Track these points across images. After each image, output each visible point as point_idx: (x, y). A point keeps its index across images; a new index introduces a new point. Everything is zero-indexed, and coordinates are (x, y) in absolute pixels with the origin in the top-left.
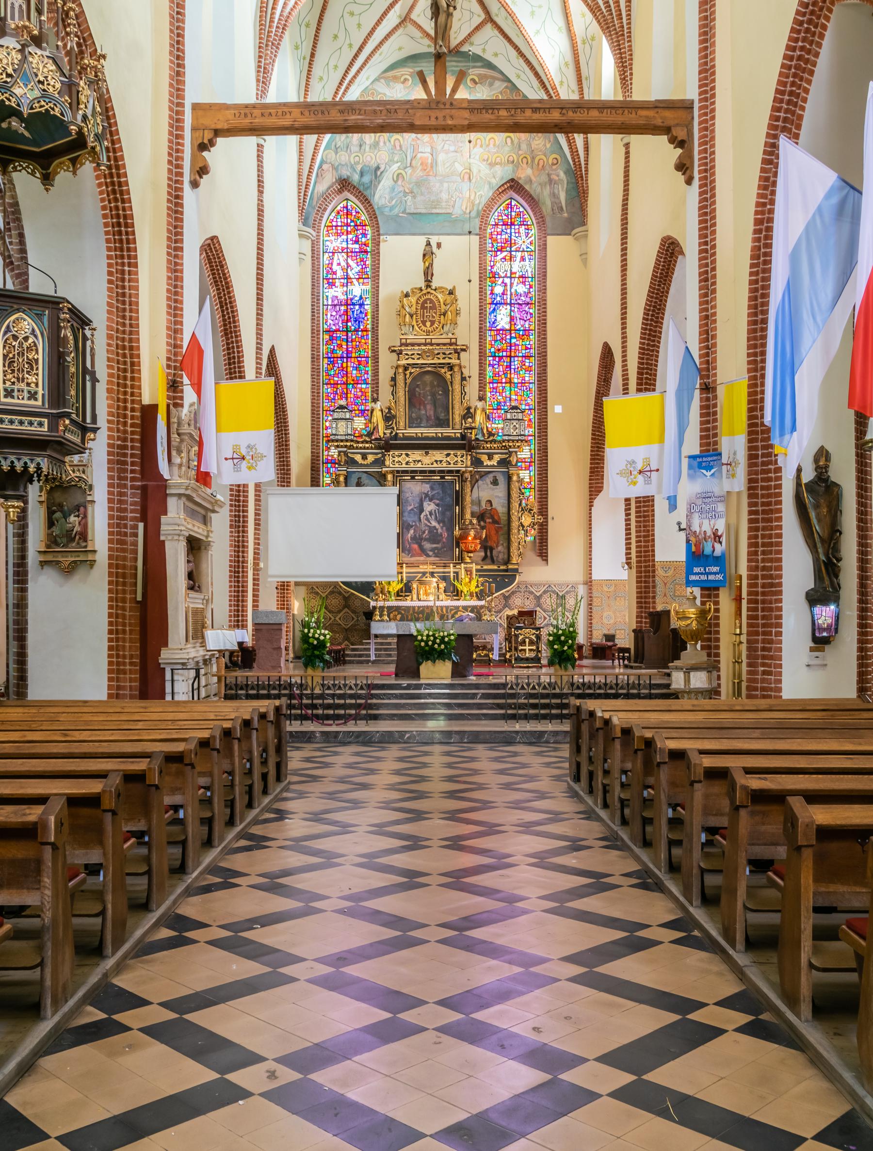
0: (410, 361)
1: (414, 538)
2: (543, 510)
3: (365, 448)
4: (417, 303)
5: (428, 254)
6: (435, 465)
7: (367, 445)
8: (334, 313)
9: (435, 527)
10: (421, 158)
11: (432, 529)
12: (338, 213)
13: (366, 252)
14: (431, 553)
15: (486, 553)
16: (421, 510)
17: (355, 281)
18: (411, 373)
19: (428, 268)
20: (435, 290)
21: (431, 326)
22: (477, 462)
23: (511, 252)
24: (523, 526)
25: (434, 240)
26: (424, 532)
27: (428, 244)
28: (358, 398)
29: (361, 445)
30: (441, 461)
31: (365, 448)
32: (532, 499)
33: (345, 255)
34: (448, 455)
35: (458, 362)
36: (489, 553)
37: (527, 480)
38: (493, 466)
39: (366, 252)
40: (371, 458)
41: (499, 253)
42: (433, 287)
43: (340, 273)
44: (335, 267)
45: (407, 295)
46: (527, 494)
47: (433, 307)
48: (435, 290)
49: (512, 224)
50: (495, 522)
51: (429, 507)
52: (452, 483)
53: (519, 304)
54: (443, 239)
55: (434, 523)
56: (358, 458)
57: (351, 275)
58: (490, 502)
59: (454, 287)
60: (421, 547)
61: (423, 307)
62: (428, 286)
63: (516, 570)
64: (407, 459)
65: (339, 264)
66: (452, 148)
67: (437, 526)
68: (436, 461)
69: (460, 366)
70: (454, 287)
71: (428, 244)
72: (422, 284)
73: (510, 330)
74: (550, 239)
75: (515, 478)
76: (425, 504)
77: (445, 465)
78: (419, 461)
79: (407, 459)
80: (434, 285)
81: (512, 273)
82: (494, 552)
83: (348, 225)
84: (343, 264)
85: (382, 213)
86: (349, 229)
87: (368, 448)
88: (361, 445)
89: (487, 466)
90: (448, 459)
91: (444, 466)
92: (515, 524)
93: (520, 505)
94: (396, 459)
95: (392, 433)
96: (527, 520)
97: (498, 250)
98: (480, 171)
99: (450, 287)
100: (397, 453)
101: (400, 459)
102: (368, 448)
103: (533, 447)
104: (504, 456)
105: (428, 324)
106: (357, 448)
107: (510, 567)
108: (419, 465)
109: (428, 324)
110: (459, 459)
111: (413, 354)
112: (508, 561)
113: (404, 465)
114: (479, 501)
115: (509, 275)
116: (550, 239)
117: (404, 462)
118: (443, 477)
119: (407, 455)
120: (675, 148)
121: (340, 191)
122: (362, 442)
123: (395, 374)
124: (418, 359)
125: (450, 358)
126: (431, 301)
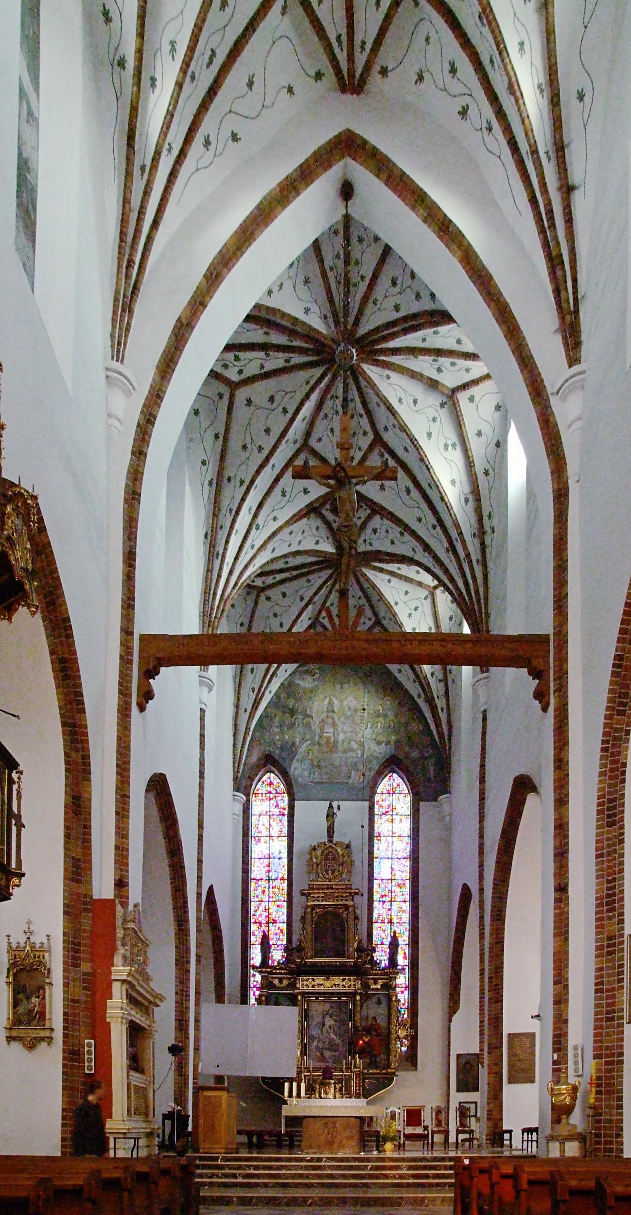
0: (316, 903)
1: (317, 1048)
2: (414, 1025)
3: (280, 974)
4: (322, 855)
5: (331, 815)
6: (334, 988)
7: (283, 971)
8: (259, 865)
9: (333, 1039)
10: (326, 737)
11: (331, 1041)
12: (263, 782)
13: (284, 815)
14: (330, 1061)
15: (371, 1059)
16: (324, 1025)
17: (275, 838)
18: (316, 912)
19: (330, 825)
20: (335, 844)
21: (332, 874)
22: (366, 986)
23: (392, 815)
24: (399, 1038)
25: (335, 804)
26: (325, 1043)
27: (331, 806)
28: (276, 934)
29: (278, 971)
30: (338, 985)
31: (280, 974)
32: (406, 1016)
33: (268, 817)
34: (344, 980)
35: (352, 903)
36: (373, 1060)
37: (402, 1001)
38: (377, 989)
39: (284, 815)
40: (285, 982)
41: (383, 816)
42: (334, 842)
43: (265, 833)
44: (261, 827)
45: (314, 849)
46: (402, 1012)
47: (334, 859)
48: (335, 844)
49: (394, 792)
50: (378, 1035)
51: (329, 1022)
52: (346, 1002)
53: (398, 858)
54: (341, 803)
55: (333, 1036)
56: (276, 982)
57: (273, 834)
58: (374, 1018)
59: (350, 842)
60: (322, 1054)
61: (326, 859)
62: (330, 841)
63: (394, 1074)
64: (313, 983)
65: (264, 825)
66: (350, 729)
67: (335, 1037)
68: (335, 985)
69: (353, 906)
70: (350, 842)
71: (331, 806)
72: (326, 840)
73: (391, 880)
74: (422, 804)
75: (394, 999)
76: (326, 1020)
77: (341, 988)
78: (322, 985)
79: (313, 983)
80: (336, 839)
81: (393, 833)
82: (378, 1059)
83: (270, 793)
84: (267, 825)
85: (296, 782)
86: (272, 796)
87: (283, 974)
88: (278, 971)
89: (373, 989)
90: (344, 983)
91: (341, 989)
92: (394, 1036)
93: (398, 1020)
94: (305, 983)
95: (301, 962)
96: (402, 1033)
97: (383, 814)
98: (369, 748)
99: (347, 842)
100: (305, 978)
101: (307, 983)
102: (283, 974)
103: (407, 975)
104: (385, 981)
105: (330, 872)
106: (275, 974)
107: (389, 1071)
108: (322, 988)
109: (330, 872)
110: (352, 983)
111: (318, 897)
112: (388, 1066)
113: (310, 988)
114: (367, 1017)
115: (391, 834)
116: (422, 804)
117: (310, 986)
118: (339, 998)
119: (313, 980)
120: (533, 679)
121: (265, 765)
122: (279, 969)
123: (305, 913)
124: (322, 901)
125: (346, 900)
126: (333, 854)
